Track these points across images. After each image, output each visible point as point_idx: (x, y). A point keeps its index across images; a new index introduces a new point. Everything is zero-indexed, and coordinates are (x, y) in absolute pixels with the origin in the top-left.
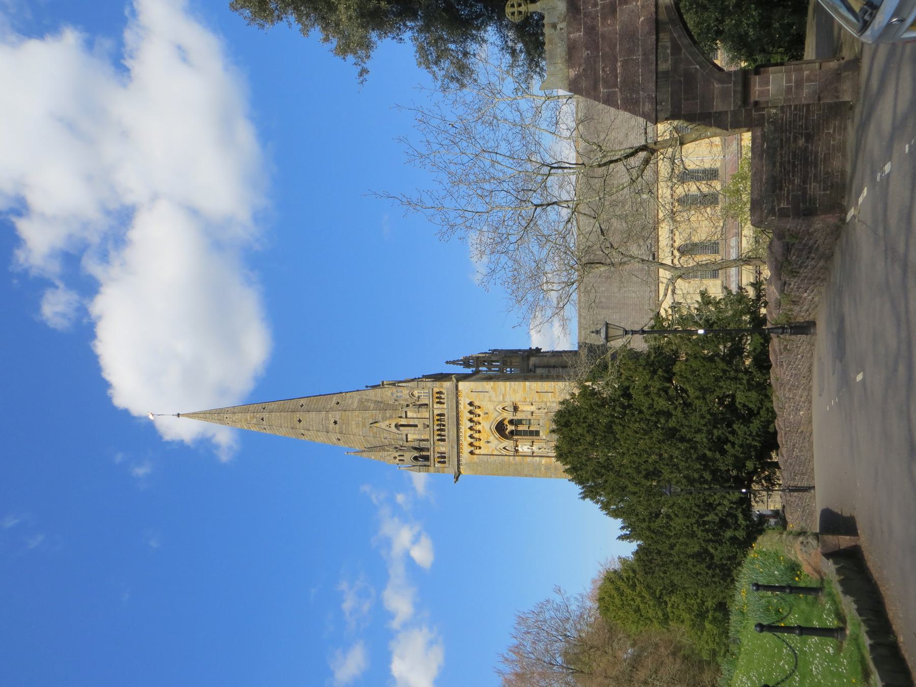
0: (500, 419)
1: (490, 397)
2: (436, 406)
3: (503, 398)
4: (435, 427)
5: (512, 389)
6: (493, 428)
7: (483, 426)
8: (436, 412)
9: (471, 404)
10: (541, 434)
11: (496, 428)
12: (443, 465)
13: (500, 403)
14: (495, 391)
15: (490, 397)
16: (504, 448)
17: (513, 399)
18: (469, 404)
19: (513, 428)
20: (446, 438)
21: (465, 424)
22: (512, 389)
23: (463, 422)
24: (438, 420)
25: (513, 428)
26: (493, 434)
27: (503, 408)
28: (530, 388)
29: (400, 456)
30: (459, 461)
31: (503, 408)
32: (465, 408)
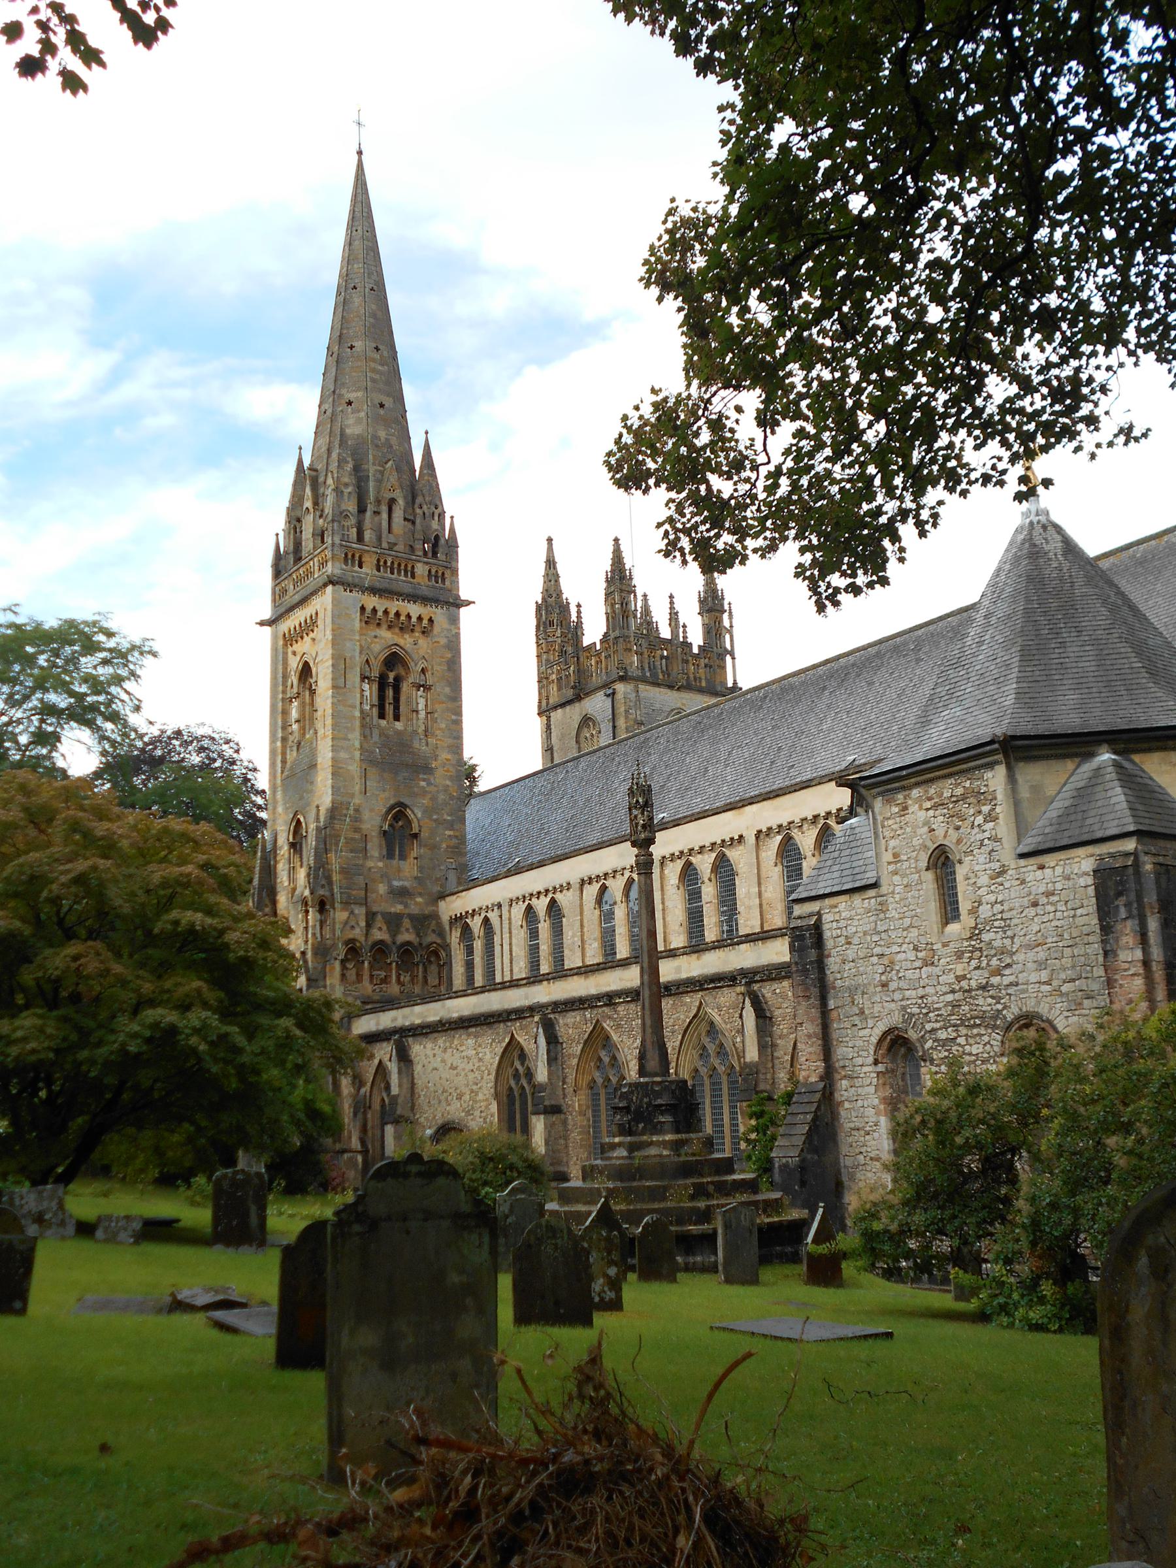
9: (431, 620)
25: (391, 680)
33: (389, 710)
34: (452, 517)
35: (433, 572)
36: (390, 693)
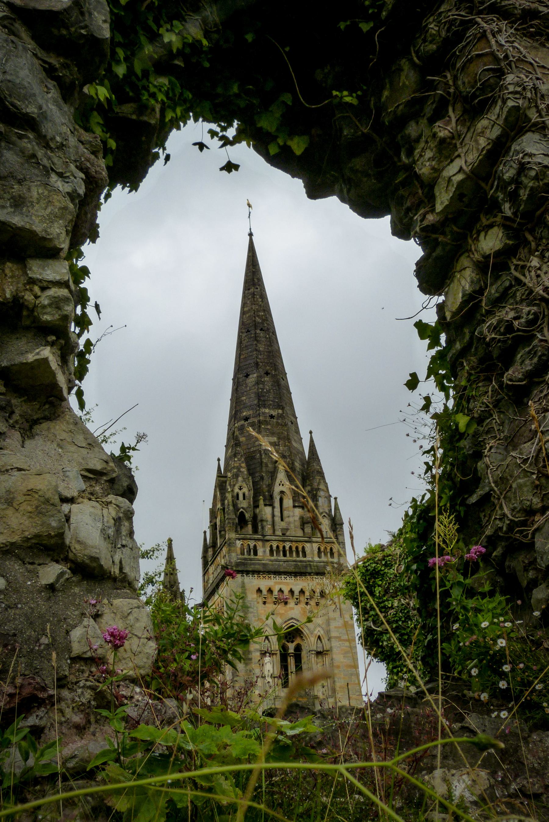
1: (335, 619)
2: (315, 546)
3: (336, 637)
4: (288, 543)
6: (291, 623)
8: (308, 546)
13: (328, 632)
15: (335, 619)
17: (335, 650)
19: (291, 650)
20: (275, 557)
21: (297, 584)
24: (297, 548)
25: (291, 650)
26: (286, 622)
27: (319, 637)
29: (244, 495)
30: (247, 572)
31: (319, 637)
34: (336, 499)
35: (322, 549)
36: (291, 662)
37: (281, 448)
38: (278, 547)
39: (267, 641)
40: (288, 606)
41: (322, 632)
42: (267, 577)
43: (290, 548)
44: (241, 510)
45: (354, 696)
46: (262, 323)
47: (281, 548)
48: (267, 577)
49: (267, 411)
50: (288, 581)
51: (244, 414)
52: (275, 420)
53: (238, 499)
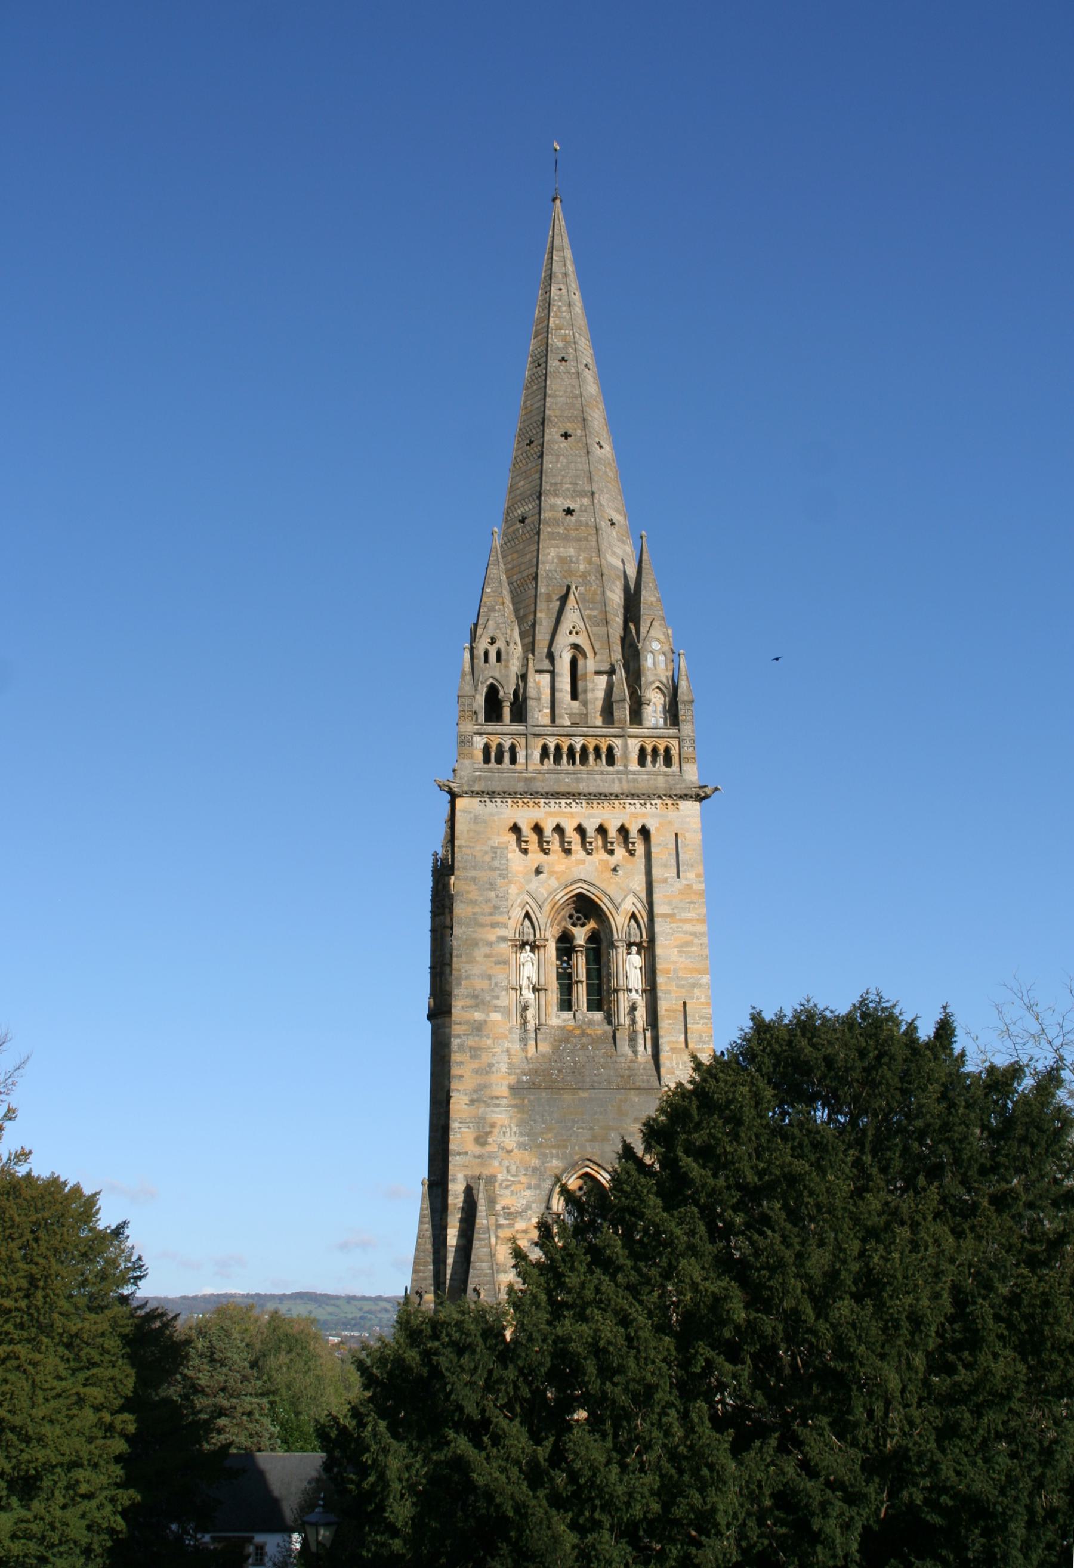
0: (605, 905)
2: (634, 745)
4: (577, 739)
5: (689, 938)
7: (583, 862)
9: (644, 832)
10: (567, 1015)
11: (580, 894)
12: (480, 756)
14: (681, 892)
15: (665, 881)
16: (527, 915)
18: (643, 827)
22: (690, 938)
23: (595, 811)
26: (567, 886)
28: (694, 986)
29: (499, 654)
30: (492, 795)
32: (635, 815)
33: (581, 994)
37: (582, 567)
38: (558, 748)
39: (527, 923)
40: (573, 857)
41: (639, 906)
42: (531, 804)
43: (584, 748)
44: (491, 680)
45: (695, 1027)
46: (565, 348)
47: (565, 749)
48: (531, 804)
49: (559, 501)
50: (574, 810)
51: (519, 512)
52: (573, 518)
53: (486, 660)
